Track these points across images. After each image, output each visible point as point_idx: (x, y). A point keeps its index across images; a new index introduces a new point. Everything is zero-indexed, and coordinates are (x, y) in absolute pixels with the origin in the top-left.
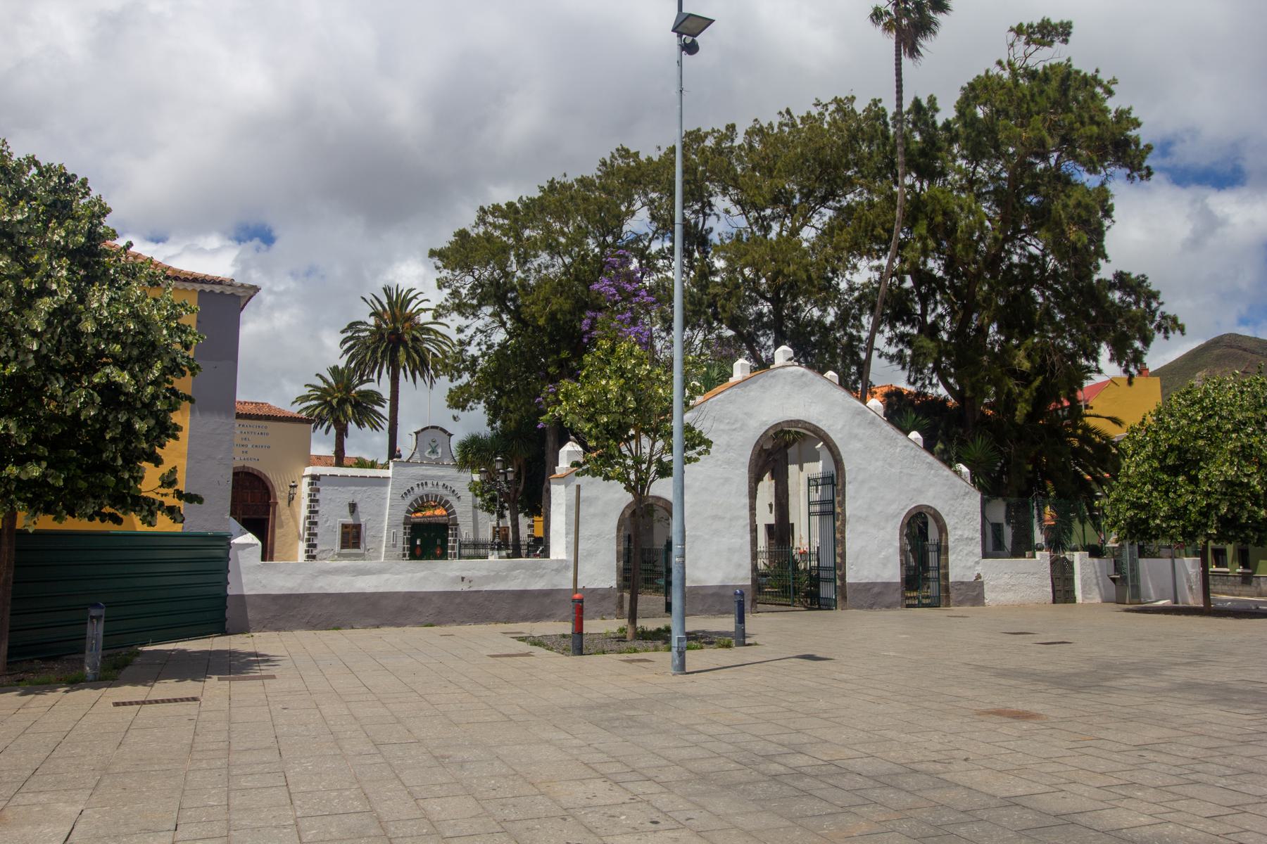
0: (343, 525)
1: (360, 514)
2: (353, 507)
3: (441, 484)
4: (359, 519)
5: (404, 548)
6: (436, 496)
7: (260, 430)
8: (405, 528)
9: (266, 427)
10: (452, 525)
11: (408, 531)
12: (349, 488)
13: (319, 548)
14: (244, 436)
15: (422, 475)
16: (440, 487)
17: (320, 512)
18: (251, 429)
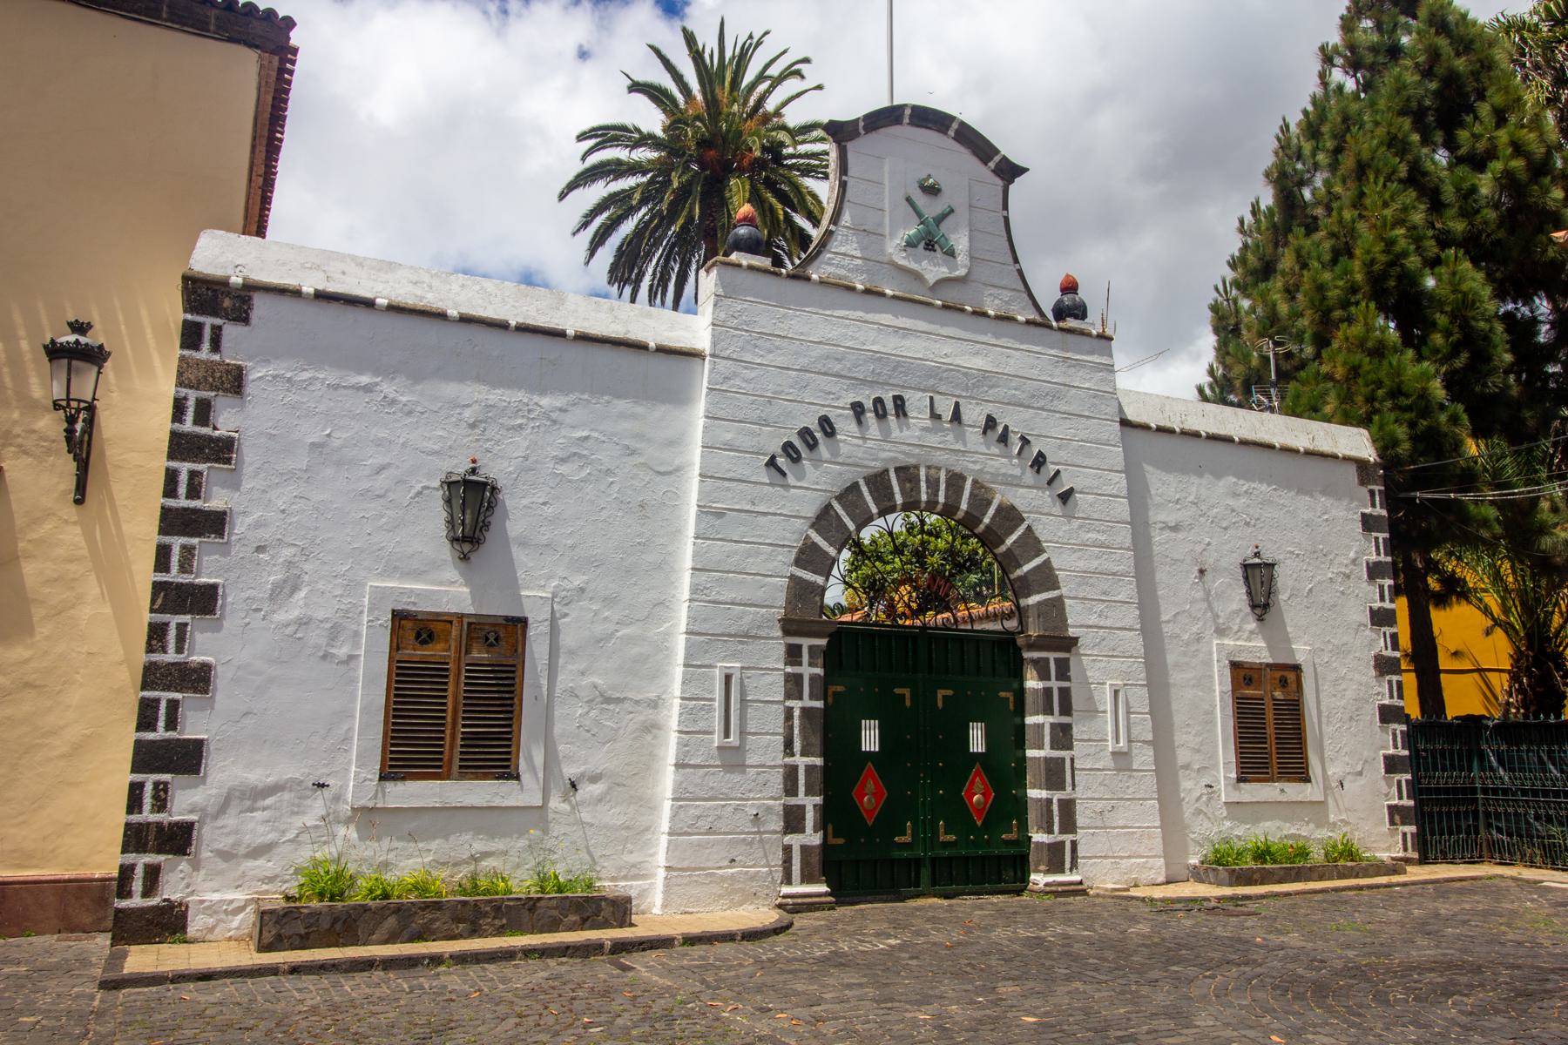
0: (399, 617)
1: (518, 554)
3: (974, 414)
4: (512, 585)
5: (791, 774)
6: (956, 480)
8: (793, 654)
10: (1043, 643)
11: (809, 670)
12: (450, 389)
13: (222, 772)
15: (879, 358)
16: (974, 436)
17: (239, 527)
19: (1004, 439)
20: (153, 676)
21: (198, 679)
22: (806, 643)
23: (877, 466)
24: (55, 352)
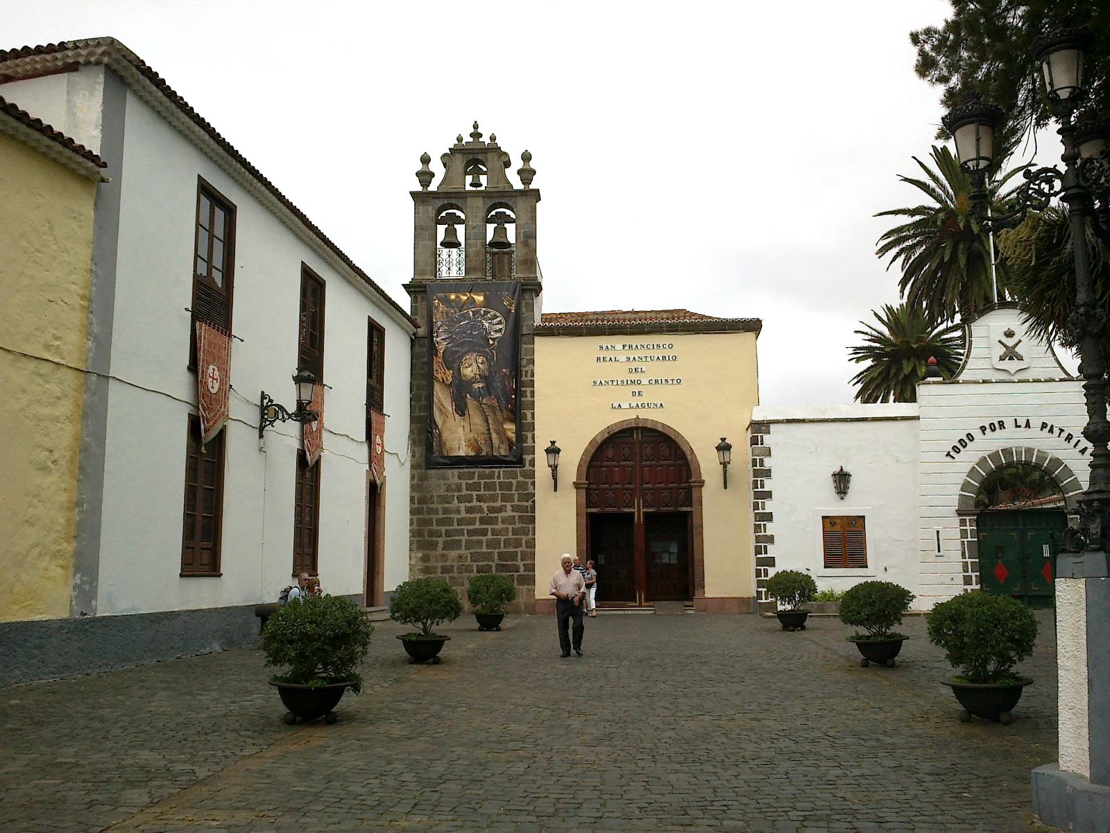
2: (842, 480)
3: (1036, 423)
5: (965, 565)
7: (660, 353)
8: (963, 523)
9: (670, 347)
14: (633, 365)
18: (642, 353)
19: (1051, 431)
20: (758, 539)
21: (771, 539)
23: (994, 450)
24: (719, 448)
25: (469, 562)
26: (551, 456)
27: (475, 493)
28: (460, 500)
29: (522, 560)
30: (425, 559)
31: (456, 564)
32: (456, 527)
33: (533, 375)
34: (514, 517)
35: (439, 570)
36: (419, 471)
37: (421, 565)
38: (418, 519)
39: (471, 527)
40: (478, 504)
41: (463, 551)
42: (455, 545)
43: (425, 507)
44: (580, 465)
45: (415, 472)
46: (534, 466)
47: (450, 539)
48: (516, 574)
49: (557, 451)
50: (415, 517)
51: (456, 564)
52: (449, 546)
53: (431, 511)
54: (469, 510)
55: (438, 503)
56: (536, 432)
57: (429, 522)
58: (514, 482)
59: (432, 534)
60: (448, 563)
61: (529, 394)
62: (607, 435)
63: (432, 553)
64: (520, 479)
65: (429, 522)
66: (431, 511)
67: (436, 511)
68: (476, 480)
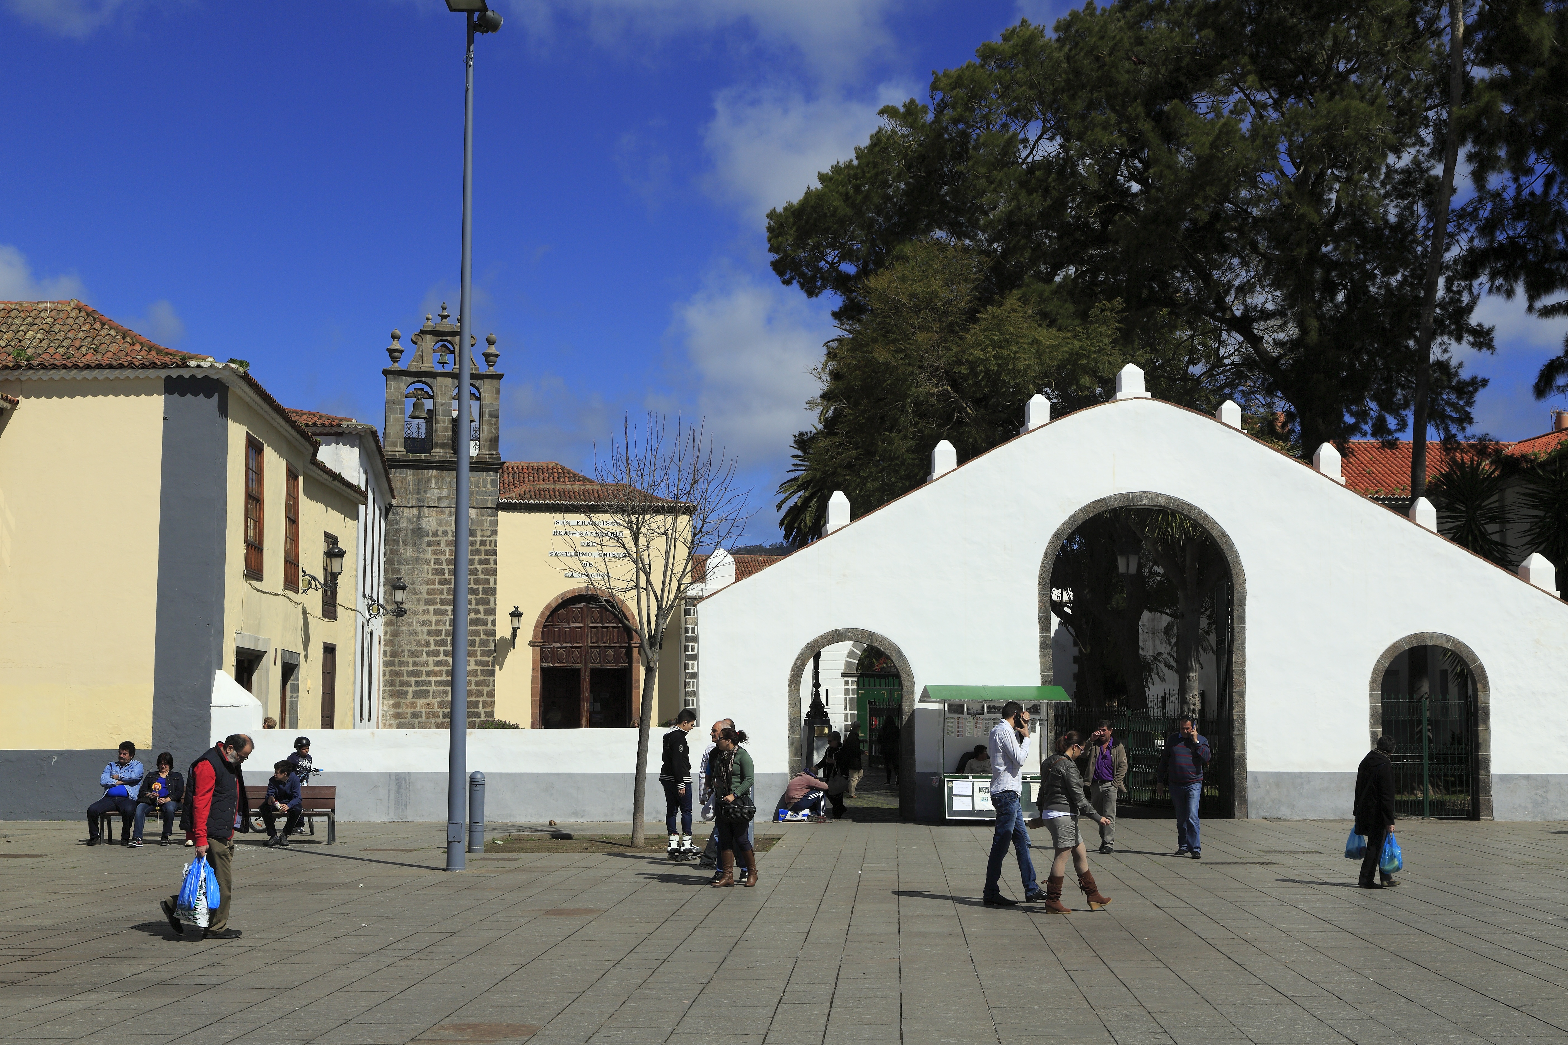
8: (847, 683)
11: (852, 687)
22: (850, 680)
25: (436, 709)
26: (516, 620)
27: (442, 649)
28: (429, 654)
29: (483, 707)
30: (396, 705)
31: (424, 711)
32: (424, 678)
33: (496, 545)
34: (476, 671)
35: (409, 716)
36: (392, 628)
37: (393, 711)
38: (390, 671)
39: (438, 679)
40: (445, 658)
41: (430, 700)
42: (425, 694)
43: (396, 659)
44: (536, 626)
45: (388, 629)
46: (495, 625)
47: (418, 689)
48: (477, 720)
49: (520, 615)
50: (388, 669)
51: (424, 711)
52: (416, 695)
53: (402, 664)
54: (438, 664)
55: (409, 656)
56: (497, 596)
57: (400, 674)
58: (477, 639)
59: (402, 684)
60: (417, 710)
61: (492, 562)
62: (560, 601)
63: (402, 701)
64: (483, 637)
65: (400, 674)
66: (402, 664)
67: (406, 664)
68: (443, 637)
